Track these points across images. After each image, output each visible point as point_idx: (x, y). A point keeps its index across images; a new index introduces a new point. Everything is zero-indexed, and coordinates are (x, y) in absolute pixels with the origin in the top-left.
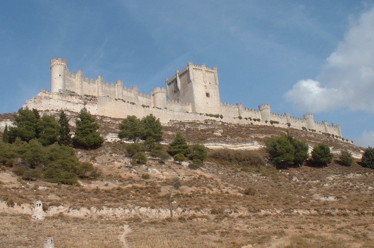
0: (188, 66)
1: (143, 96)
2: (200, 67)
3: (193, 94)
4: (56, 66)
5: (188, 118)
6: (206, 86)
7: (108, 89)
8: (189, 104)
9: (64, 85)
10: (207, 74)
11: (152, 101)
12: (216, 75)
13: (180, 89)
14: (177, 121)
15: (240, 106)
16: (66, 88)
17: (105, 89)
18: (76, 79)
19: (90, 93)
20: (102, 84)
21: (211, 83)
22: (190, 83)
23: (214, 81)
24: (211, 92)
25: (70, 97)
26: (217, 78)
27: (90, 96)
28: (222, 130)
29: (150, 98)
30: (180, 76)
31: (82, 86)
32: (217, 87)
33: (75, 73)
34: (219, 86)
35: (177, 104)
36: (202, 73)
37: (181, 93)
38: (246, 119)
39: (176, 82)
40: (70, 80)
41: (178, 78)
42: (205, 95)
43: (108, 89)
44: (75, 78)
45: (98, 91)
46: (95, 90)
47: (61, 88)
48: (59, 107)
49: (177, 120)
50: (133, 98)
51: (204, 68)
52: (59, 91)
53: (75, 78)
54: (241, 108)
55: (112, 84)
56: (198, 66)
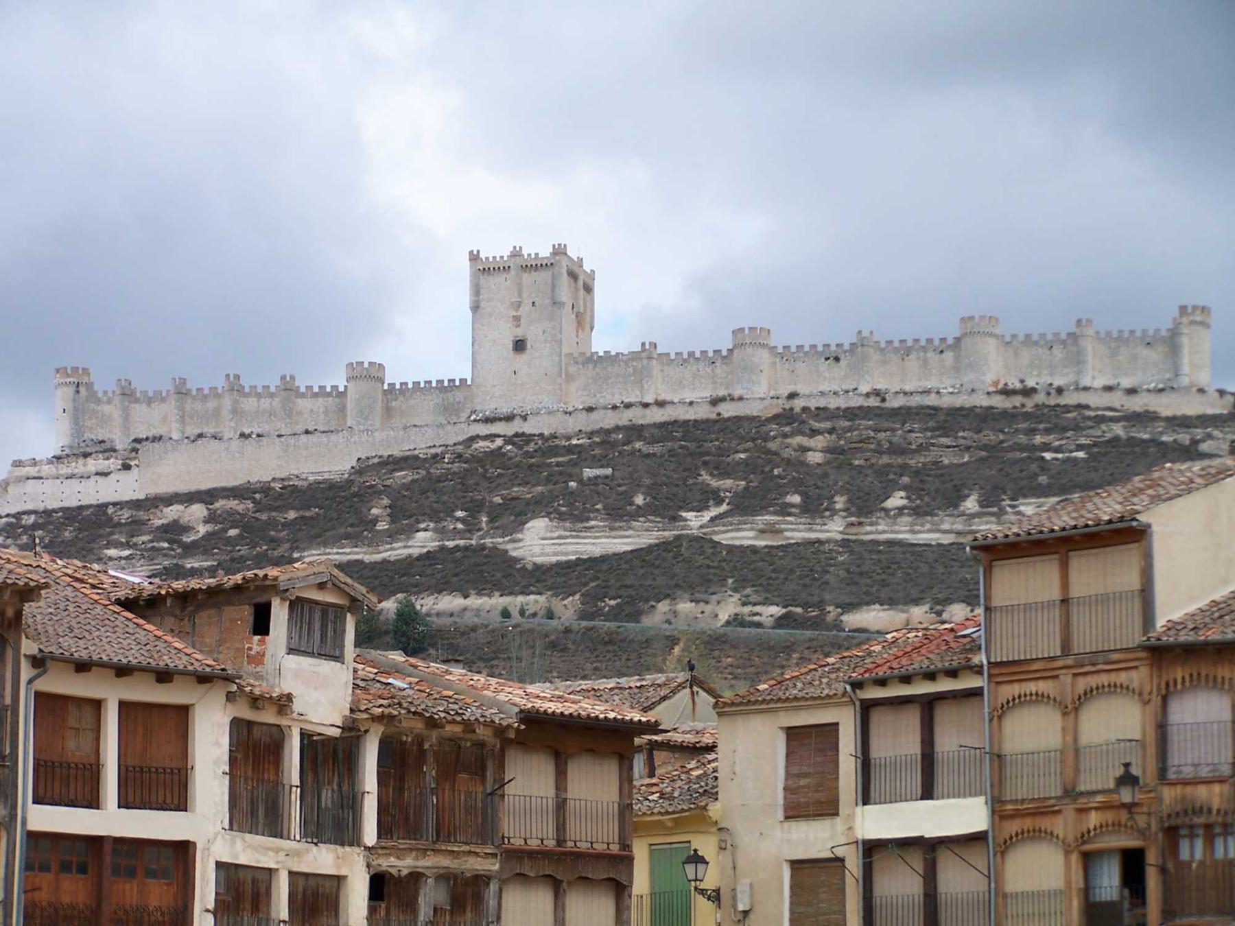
5: (414, 442)
6: (517, 319)
10: (527, 278)
14: (380, 457)
16: (88, 435)
17: (192, 409)
21: (536, 303)
24: (532, 333)
28: (386, 502)
40: (97, 412)
43: (200, 408)
46: (165, 419)
49: (380, 454)
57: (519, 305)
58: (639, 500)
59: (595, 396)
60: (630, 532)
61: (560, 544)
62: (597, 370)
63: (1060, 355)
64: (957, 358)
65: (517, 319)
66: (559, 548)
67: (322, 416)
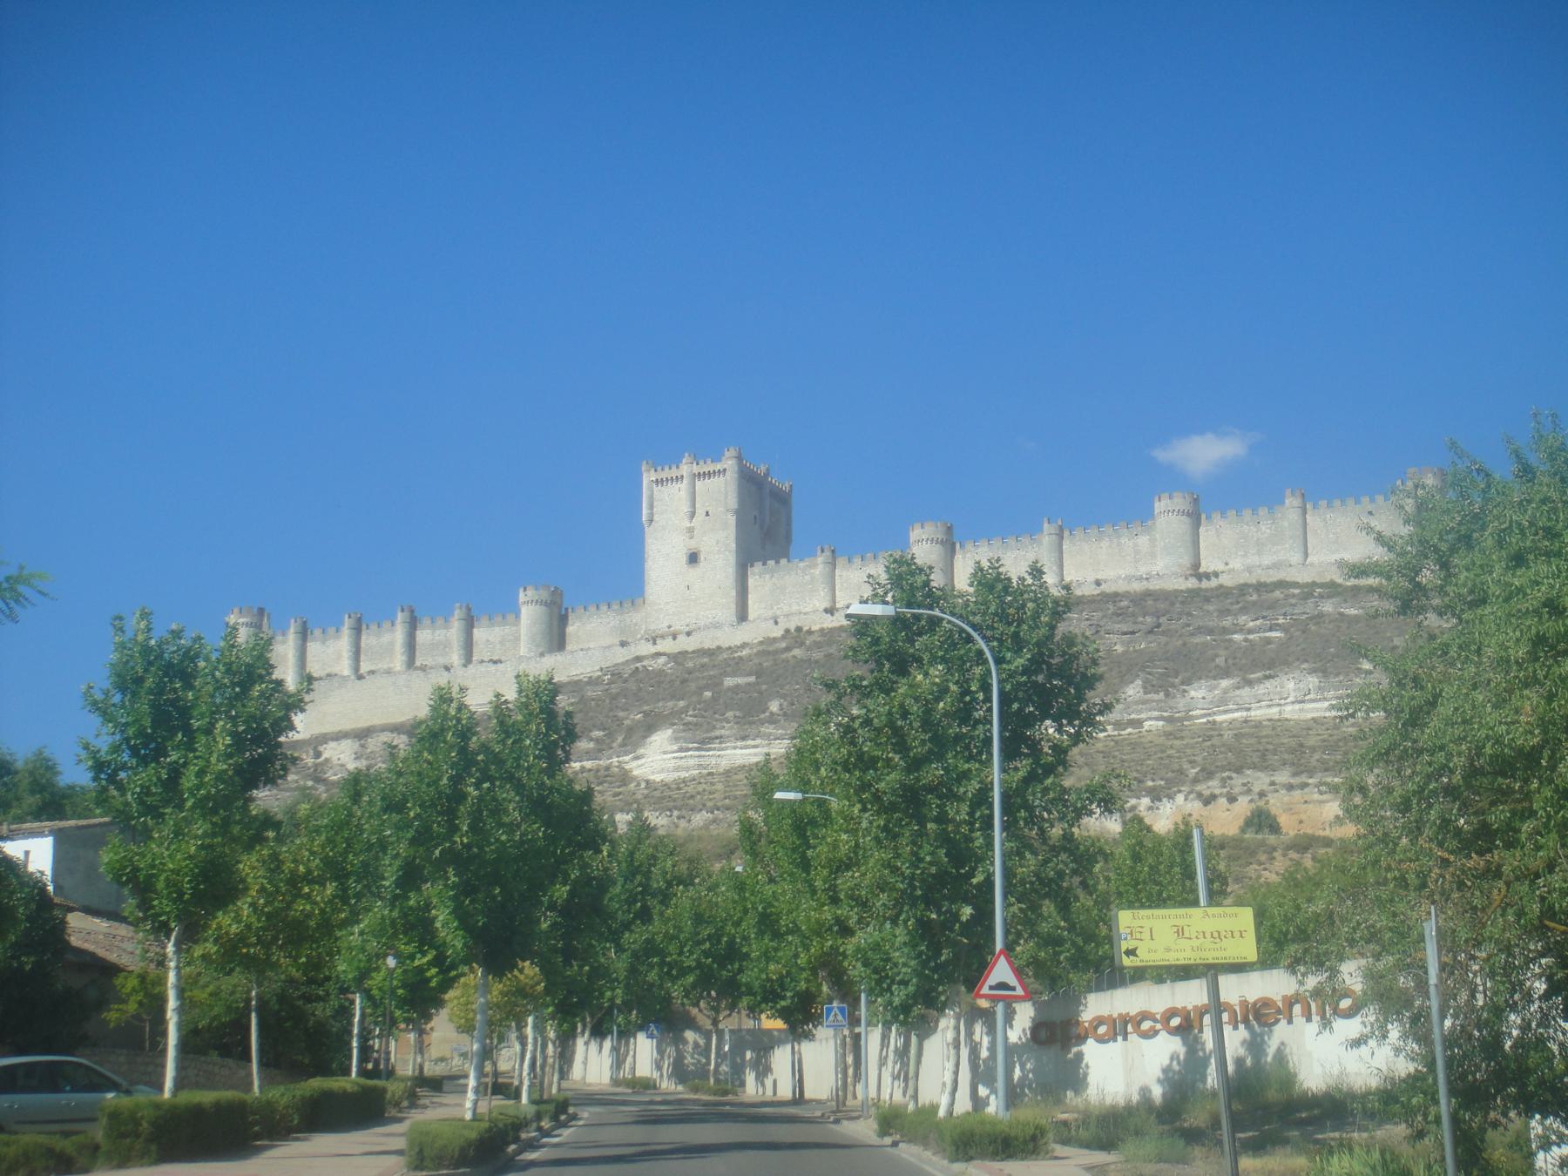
6: (691, 530)
10: (699, 484)
42: (684, 559)
56: (667, 468)
57: (693, 515)
58: (774, 706)
59: (772, 608)
60: (758, 741)
61: (682, 758)
63: (1268, 531)
64: (1153, 541)
65: (691, 530)
66: (682, 762)
67: (498, 647)
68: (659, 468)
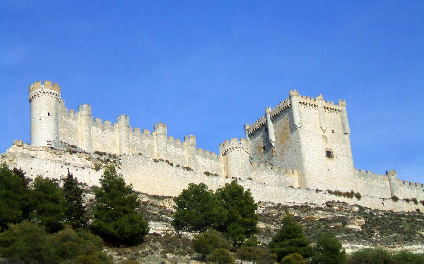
0: (290, 97)
1: (205, 156)
2: (313, 99)
3: (300, 151)
4: (40, 95)
5: (293, 198)
6: (325, 138)
7: (139, 142)
8: (293, 172)
9: (57, 133)
11: (222, 165)
12: (345, 115)
13: (273, 144)
14: (273, 203)
15: (393, 177)
16: (61, 139)
17: (133, 142)
18: (79, 121)
19: (105, 149)
20: (127, 132)
21: (334, 132)
22: (295, 133)
23: (341, 128)
25: (68, 154)
26: (347, 122)
27: (105, 154)
29: (218, 160)
30: (274, 118)
31: (90, 136)
32: (348, 140)
33: (77, 110)
34: (350, 136)
35: (270, 171)
36: (317, 111)
37: (277, 150)
38: (407, 201)
39: (267, 130)
40: (68, 124)
41: (270, 123)
42: (324, 154)
43: (139, 142)
44: (75, 119)
45: (120, 145)
46: (114, 143)
47: (51, 137)
48: (48, 173)
49: (272, 201)
50: (187, 159)
51: (320, 102)
52: (48, 144)
53: (75, 119)
54: (394, 181)
55: (147, 132)
56: (309, 98)
62: (366, 180)
68: (304, 97)
